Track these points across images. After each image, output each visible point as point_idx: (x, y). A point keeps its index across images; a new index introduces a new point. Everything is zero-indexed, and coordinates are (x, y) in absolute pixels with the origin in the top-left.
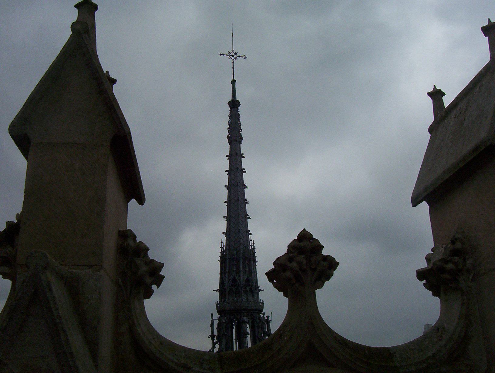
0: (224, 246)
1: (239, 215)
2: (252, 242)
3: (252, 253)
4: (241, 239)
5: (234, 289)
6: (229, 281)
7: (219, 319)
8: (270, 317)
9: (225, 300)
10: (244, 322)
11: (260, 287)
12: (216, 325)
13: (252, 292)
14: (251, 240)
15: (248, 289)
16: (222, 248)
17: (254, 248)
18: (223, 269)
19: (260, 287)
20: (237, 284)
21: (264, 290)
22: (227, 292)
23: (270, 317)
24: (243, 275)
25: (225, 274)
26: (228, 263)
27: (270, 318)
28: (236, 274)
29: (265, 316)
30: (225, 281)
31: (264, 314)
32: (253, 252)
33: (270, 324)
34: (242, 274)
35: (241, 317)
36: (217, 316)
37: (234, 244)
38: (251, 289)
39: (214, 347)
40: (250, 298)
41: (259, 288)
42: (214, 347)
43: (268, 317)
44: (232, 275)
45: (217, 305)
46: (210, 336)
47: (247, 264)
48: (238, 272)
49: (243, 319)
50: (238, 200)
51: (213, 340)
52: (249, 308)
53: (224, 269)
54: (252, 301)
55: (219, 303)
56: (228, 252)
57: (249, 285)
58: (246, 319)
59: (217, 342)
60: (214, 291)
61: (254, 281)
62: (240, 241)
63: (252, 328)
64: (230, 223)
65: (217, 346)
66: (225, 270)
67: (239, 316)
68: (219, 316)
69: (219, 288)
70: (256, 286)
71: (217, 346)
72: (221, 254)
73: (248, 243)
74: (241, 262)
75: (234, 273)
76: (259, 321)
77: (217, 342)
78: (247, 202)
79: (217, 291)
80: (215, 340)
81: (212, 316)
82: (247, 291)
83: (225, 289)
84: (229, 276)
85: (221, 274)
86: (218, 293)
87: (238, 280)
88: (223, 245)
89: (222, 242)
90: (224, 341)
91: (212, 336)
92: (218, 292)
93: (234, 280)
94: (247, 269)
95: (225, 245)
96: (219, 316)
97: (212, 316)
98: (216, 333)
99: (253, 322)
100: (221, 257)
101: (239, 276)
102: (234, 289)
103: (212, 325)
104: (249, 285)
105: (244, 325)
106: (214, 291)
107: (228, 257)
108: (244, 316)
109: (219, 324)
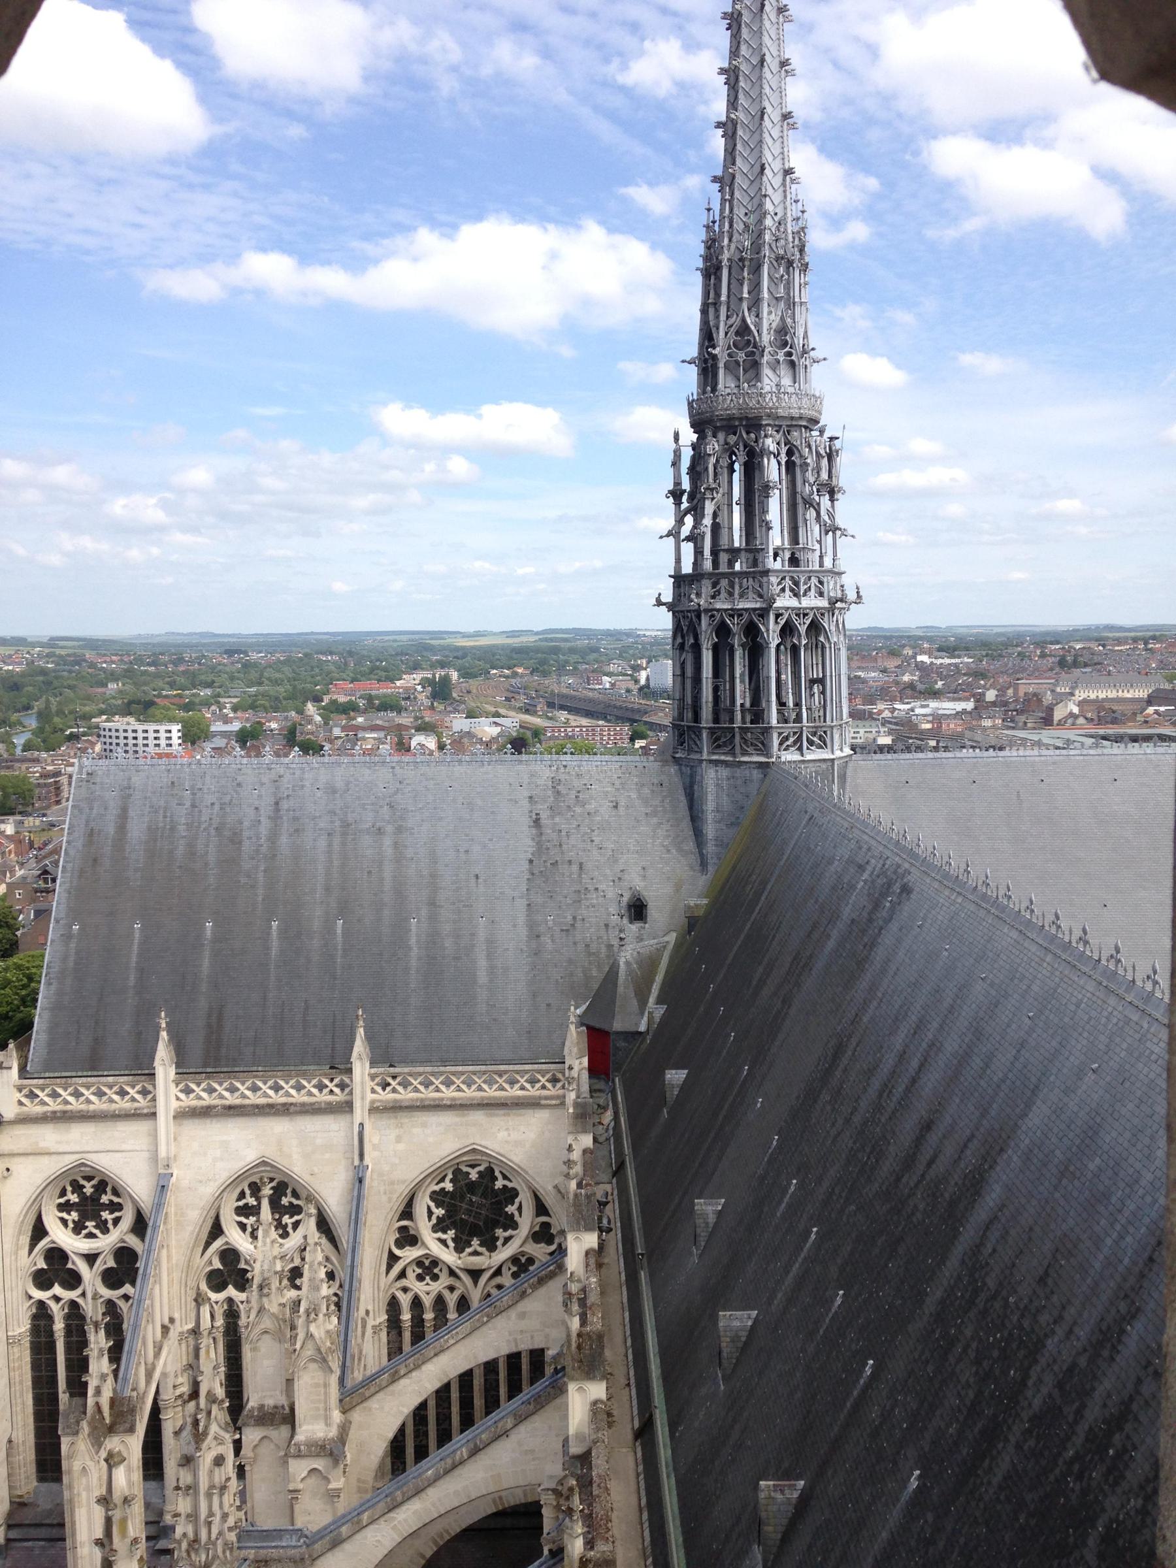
0: (714, 222)
1: (763, 114)
2: (800, 204)
3: (797, 242)
4: (765, 196)
5: (741, 356)
6: (726, 334)
7: (694, 447)
8: (837, 438)
9: (714, 390)
10: (764, 452)
11: (813, 349)
12: (685, 463)
13: (792, 364)
14: (796, 201)
15: (781, 356)
16: (707, 227)
17: (803, 229)
18: (712, 295)
19: (813, 349)
20: (749, 341)
21: (825, 359)
22: (721, 365)
23: (837, 438)
24: (770, 313)
25: (717, 311)
26: (725, 273)
27: (837, 444)
28: (749, 309)
29: (827, 435)
30: (714, 330)
31: (822, 432)
32: (800, 239)
33: (838, 459)
34: (765, 310)
35: (756, 441)
36: (689, 436)
37: (746, 214)
38: (789, 354)
39: (680, 522)
40: (786, 381)
41: (812, 353)
42: (680, 522)
43: (831, 439)
44: (737, 315)
45: (690, 404)
46: (670, 492)
47: (782, 276)
48: (755, 303)
49: (763, 443)
50: (762, 61)
51: (678, 503)
52: (781, 412)
53: (712, 295)
54: (791, 390)
55: (695, 397)
56: (726, 241)
57: (785, 344)
58: (771, 445)
59: (687, 512)
60: (683, 361)
61: (800, 332)
62: (761, 205)
63: (790, 466)
64: (735, 145)
65: (689, 520)
66: (718, 295)
67: (753, 436)
68: (696, 435)
69: (696, 354)
70: (804, 345)
71: (689, 520)
72: (708, 248)
73: (789, 210)
74: (765, 269)
75: (745, 306)
76: (807, 450)
77: (687, 512)
78: (786, 71)
79: (690, 363)
80: (685, 505)
81: (676, 437)
82: (778, 362)
83: (714, 357)
84: (728, 317)
85: (704, 311)
86: (693, 372)
87: (752, 327)
88: (711, 219)
89: (709, 210)
90: (709, 508)
91: (676, 494)
92: (693, 365)
93: (744, 330)
94: (781, 292)
95: (717, 218)
96: (696, 435)
97: (676, 437)
98: (686, 485)
99: (790, 453)
100: (707, 258)
101: (757, 316)
102: (741, 356)
103: (676, 464)
104: (785, 344)
105: (766, 460)
106: (683, 361)
107: (725, 256)
108: (766, 436)
109: (693, 458)
